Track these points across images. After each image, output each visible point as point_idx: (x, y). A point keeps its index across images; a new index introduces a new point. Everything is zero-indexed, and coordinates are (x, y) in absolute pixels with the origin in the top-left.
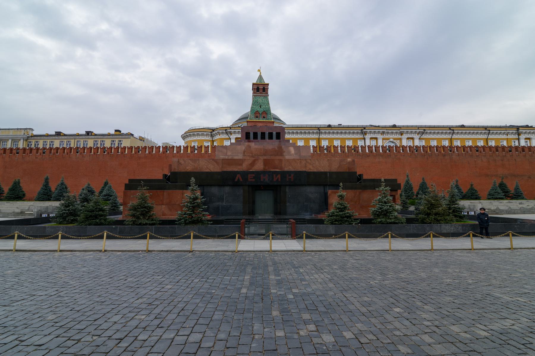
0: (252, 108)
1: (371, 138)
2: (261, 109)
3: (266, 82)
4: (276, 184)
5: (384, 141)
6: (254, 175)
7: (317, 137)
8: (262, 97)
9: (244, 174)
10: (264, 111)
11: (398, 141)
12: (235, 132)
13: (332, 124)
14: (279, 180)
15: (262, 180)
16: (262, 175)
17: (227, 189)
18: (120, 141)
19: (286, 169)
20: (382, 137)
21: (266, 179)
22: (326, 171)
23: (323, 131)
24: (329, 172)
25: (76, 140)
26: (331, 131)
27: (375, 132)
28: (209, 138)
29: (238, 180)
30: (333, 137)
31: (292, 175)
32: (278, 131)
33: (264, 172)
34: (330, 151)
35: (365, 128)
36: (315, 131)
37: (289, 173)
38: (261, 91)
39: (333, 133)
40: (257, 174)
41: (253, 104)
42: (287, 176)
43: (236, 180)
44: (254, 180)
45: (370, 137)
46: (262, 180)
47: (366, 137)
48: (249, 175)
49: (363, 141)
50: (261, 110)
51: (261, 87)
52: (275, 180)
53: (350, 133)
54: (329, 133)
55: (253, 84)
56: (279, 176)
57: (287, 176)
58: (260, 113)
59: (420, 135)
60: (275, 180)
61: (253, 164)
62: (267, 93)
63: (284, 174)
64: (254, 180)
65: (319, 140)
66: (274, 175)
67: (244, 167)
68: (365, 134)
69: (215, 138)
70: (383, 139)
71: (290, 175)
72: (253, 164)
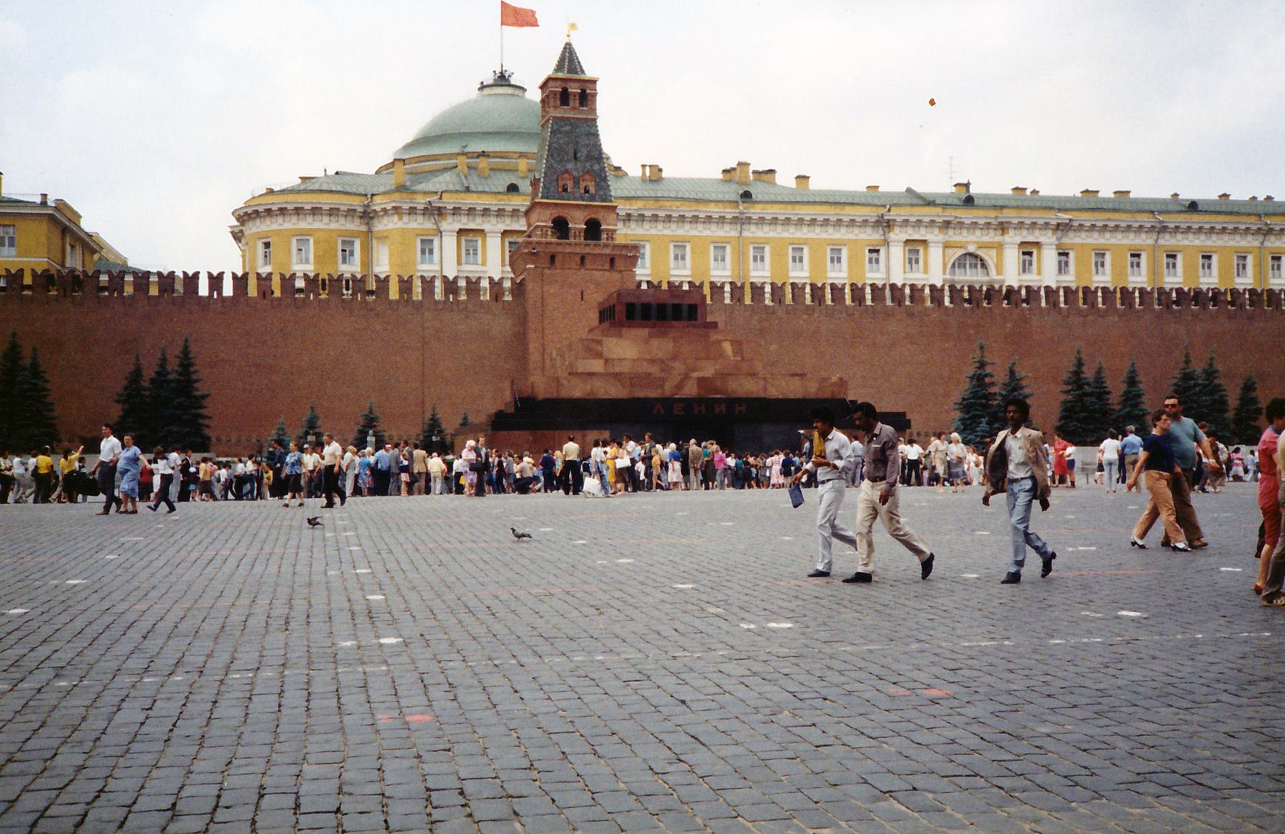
5: (950, 251)
9: (668, 402)
11: (993, 252)
33: (699, 400)
37: (740, 401)
38: (574, 102)
40: (688, 402)
56: (723, 406)
59: (1059, 233)
60: (717, 411)
61: (679, 386)
62: (594, 110)
67: (668, 390)
68: (888, 225)
70: (947, 246)
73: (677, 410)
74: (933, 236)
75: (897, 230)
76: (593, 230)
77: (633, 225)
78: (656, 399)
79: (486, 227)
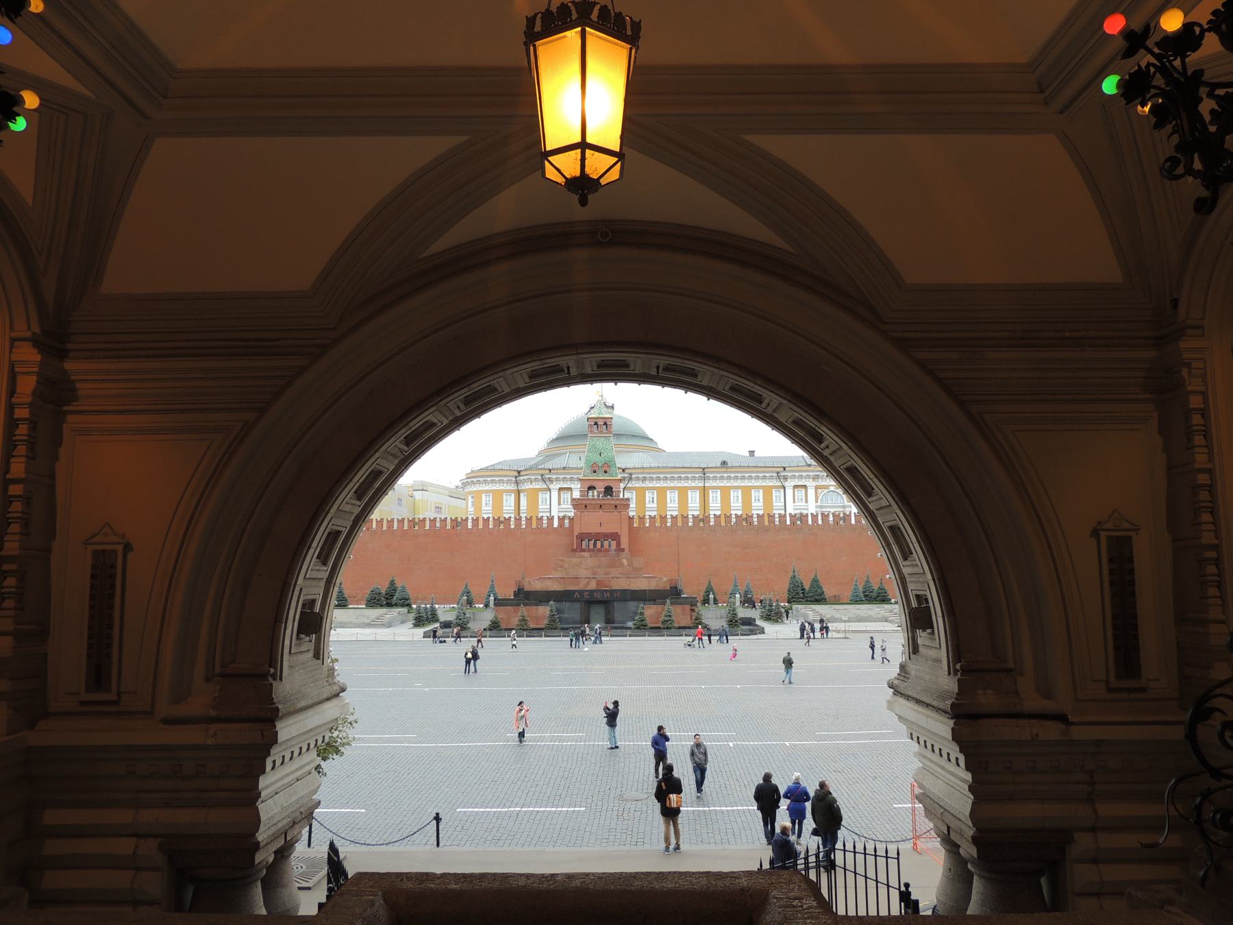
1: (795, 487)
9: (581, 592)
12: (557, 479)
20: (814, 484)
21: (598, 596)
27: (801, 477)
28: (513, 487)
37: (616, 591)
40: (591, 592)
50: (600, 460)
53: (757, 478)
61: (588, 584)
63: (612, 592)
65: (704, 491)
68: (786, 478)
69: (522, 487)
70: (817, 488)
72: (588, 584)
74: (810, 483)
76: (609, 490)
79: (572, 486)
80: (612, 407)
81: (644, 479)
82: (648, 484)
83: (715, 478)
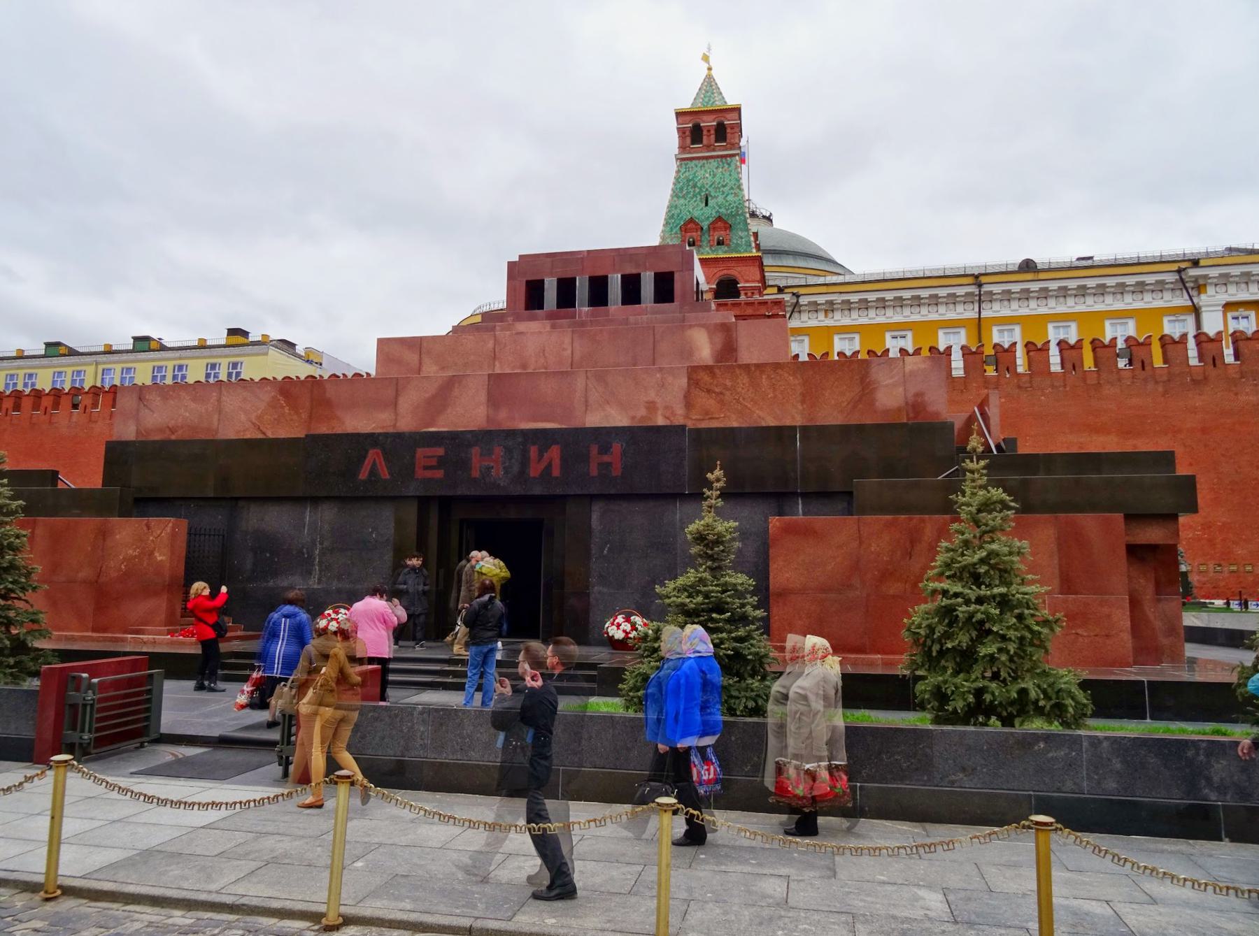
0: (670, 207)
1: (1228, 306)
2: (708, 211)
3: (731, 102)
4: (537, 491)
6: (440, 451)
7: (970, 313)
8: (714, 163)
9: (397, 445)
10: (719, 219)
13: (1041, 257)
14: (556, 472)
15: (476, 474)
16: (475, 451)
17: (327, 515)
18: (235, 365)
19: (594, 420)
21: (493, 471)
22: (788, 422)
23: (997, 289)
24: (805, 429)
25: (101, 368)
26: (1035, 287)
29: (373, 472)
30: (1043, 310)
31: (617, 447)
32: (664, 267)
33: (485, 437)
34: (1011, 367)
35: (1195, 263)
36: (961, 291)
37: (603, 436)
39: (1044, 294)
41: (676, 194)
42: (594, 450)
43: (363, 475)
44: (439, 474)
45: (1224, 298)
46: (476, 474)
47: (1203, 300)
48: (420, 452)
49: (1191, 320)
50: (705, 215)
51: (709, 123)
52: (534, 471)
54: (1026, 295)
55: (680, 114)
56: (554, 453)
57: (594, 450)
58: (705, 225)
60: (534, 471)
63: (578, 443)
64: (439, 474)
66: (533, 451)
68: (1200, 287)
71: (605, 449)
73: (427, 470)
75: (1211, 290)
77: (837, 315)
78: (372, 439)
80: (768, 219)
81: (830, 308)
82: (840, 319)
83: (1008, 296)
